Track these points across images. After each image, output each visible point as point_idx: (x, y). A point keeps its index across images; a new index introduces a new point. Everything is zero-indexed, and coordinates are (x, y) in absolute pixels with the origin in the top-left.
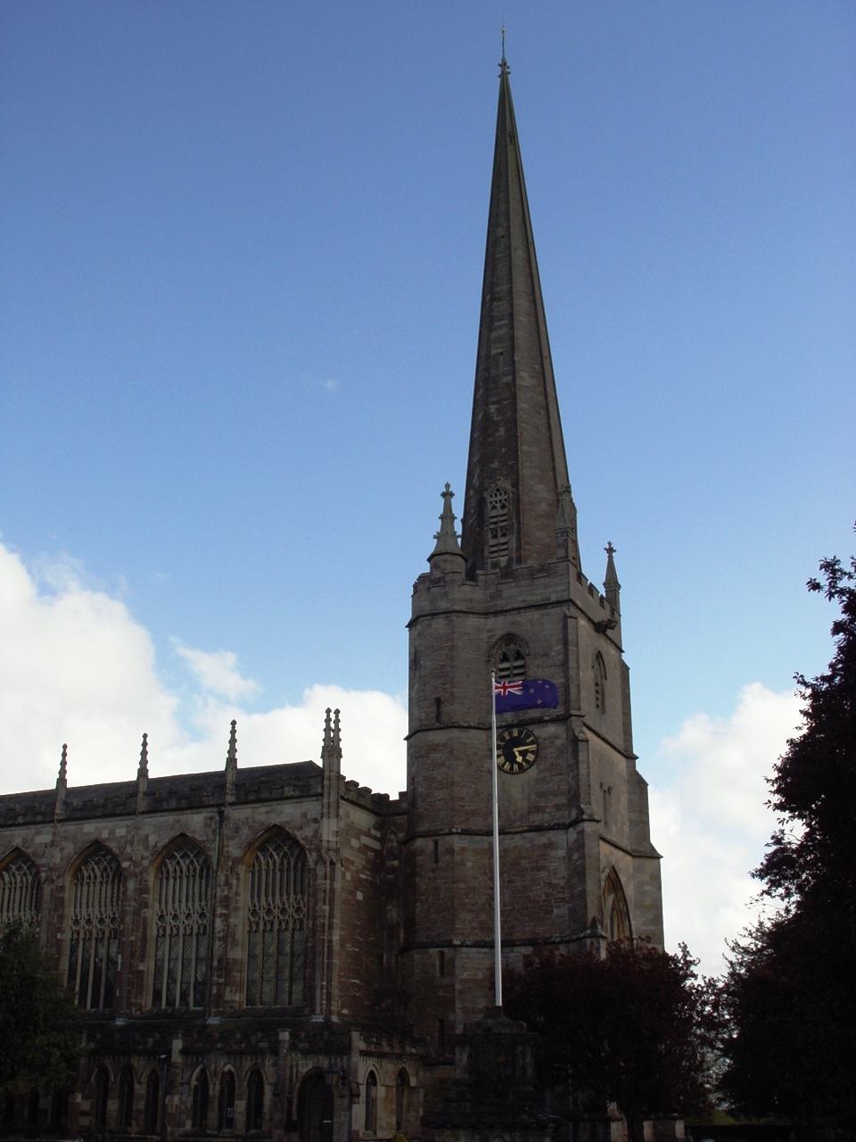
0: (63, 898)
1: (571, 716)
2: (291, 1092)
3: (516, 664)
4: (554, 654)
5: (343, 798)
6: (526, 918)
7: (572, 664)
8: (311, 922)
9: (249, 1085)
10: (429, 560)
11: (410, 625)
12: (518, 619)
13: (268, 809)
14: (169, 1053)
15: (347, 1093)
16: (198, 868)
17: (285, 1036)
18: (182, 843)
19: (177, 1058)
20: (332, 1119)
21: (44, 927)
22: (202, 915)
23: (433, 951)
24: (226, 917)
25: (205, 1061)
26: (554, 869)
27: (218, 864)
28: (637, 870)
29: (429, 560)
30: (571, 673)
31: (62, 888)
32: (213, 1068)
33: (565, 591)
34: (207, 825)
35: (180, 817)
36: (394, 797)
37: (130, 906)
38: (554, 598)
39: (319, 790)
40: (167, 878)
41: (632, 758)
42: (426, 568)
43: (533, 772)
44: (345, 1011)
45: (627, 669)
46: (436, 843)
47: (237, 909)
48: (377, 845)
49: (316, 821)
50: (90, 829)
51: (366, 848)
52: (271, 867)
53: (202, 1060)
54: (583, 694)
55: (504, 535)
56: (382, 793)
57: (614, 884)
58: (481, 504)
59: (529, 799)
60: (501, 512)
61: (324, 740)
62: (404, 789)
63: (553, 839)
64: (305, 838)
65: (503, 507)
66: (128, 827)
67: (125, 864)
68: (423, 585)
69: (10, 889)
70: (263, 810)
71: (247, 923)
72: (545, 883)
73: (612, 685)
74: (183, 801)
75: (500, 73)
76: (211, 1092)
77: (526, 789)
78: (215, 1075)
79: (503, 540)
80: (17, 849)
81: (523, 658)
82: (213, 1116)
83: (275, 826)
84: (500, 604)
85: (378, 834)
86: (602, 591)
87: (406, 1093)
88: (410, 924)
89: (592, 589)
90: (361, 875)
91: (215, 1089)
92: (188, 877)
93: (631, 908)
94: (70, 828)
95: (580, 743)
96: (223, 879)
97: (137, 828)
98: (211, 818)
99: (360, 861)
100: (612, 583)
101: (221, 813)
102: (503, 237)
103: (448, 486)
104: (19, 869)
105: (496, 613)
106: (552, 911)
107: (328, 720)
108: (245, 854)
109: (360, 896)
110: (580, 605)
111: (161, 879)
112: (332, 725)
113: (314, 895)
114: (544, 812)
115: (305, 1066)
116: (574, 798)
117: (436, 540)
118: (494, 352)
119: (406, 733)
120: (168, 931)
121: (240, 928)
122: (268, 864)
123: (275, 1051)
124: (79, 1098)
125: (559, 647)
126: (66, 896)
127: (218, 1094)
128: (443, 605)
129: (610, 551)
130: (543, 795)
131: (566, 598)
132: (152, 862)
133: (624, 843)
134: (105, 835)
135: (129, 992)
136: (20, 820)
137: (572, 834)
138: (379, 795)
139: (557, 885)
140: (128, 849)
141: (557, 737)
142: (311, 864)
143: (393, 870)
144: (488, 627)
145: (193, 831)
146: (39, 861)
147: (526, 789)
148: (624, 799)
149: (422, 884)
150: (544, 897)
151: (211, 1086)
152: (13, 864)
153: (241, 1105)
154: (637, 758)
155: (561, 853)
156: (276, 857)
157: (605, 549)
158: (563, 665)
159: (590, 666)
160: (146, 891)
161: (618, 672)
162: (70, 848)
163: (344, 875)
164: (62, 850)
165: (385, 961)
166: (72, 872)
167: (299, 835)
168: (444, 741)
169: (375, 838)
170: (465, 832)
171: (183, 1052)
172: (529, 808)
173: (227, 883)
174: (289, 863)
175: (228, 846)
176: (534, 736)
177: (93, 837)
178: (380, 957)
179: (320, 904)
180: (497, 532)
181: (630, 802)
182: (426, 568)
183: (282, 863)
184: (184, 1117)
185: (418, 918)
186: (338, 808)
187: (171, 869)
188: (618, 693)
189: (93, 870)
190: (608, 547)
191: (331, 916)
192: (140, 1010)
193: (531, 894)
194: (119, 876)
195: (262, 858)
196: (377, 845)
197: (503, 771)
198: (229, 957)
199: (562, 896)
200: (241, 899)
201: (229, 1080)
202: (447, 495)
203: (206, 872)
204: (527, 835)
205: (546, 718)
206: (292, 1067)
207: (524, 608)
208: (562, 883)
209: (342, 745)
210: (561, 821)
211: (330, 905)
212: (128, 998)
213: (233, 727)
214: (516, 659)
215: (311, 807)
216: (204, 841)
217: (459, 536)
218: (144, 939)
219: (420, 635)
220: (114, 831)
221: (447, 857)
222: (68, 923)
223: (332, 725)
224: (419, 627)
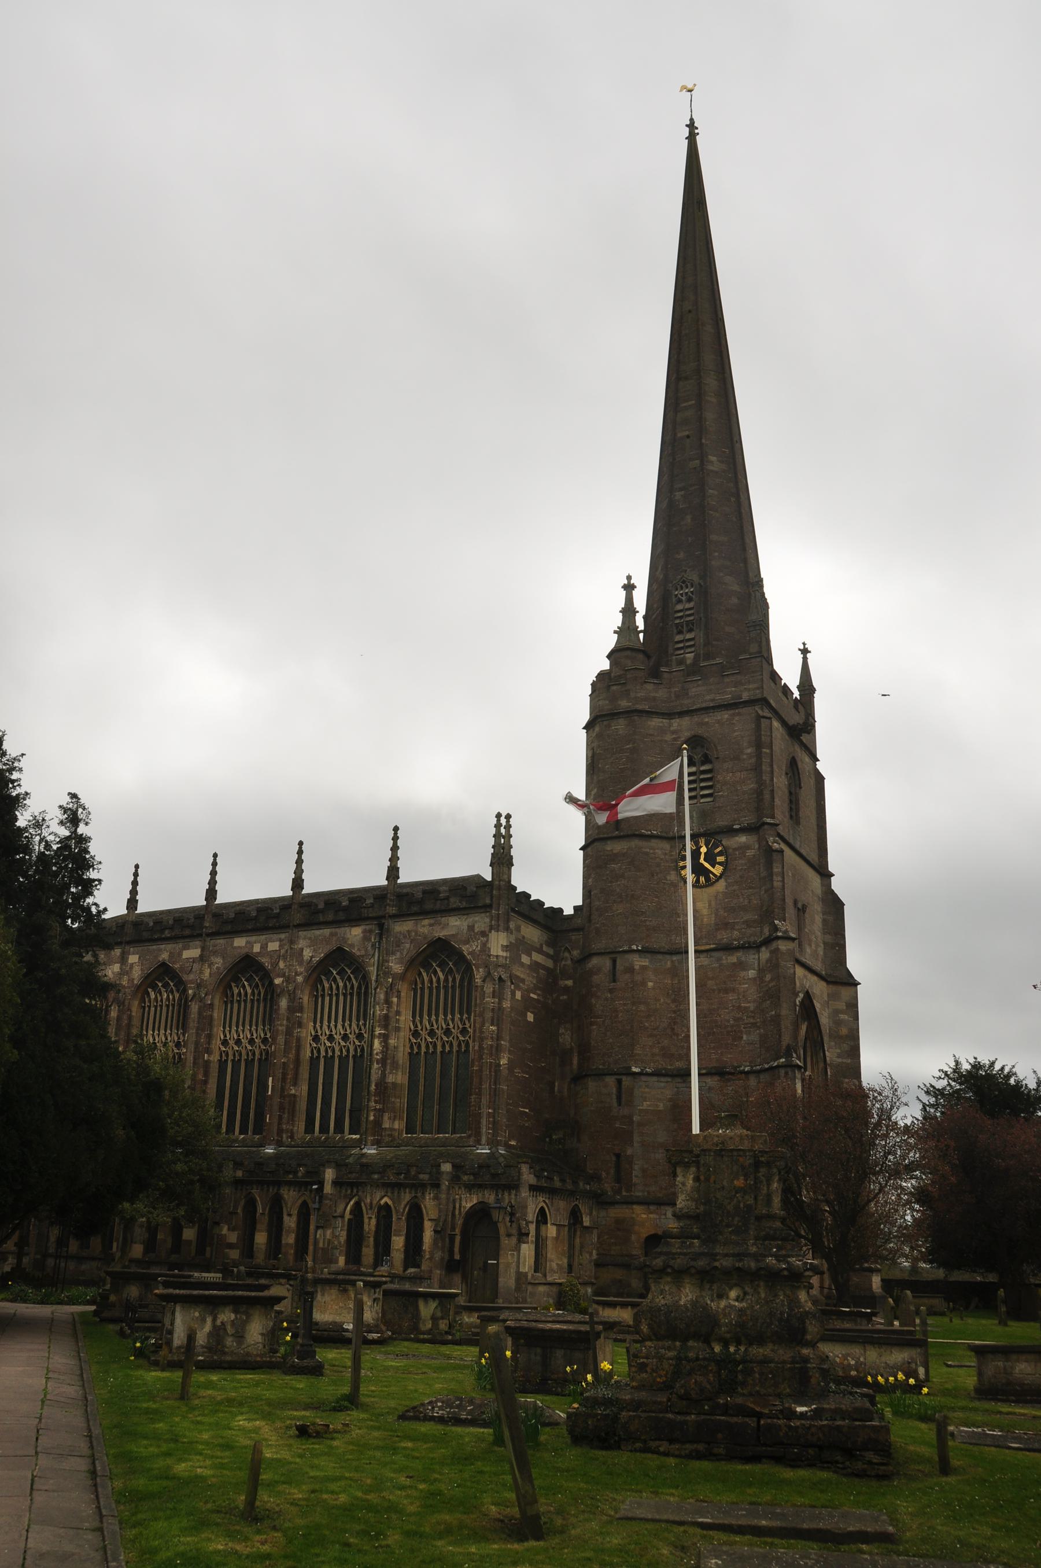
0: (211, 1016)
1: (765, 824)
2: (453, 1229)
3: (703, 768)
4: (745, 757)
5: (513, 910)
6: (712, 1045)
7: (765, 768)
8: (477, 1044)
9: (408, 1220)
10: (608, 657)
11: (588, 727)
12: (706, 720)
13: (432, 921)
14: (321, 1184)
15: (514, 1231)
16: (356, 985)
17: (446, 1167)
19: (328, 1189)
20: (498, 1260)
21: (192, 1047)
22: (360, 1037)
23: (611, 1080)
24: (385, 1038)
25: (360, 1193)
27: (376, 981)
28: (832, 996)
29: (608, 657)
30: (764, 778)
31: (211, 1005)
32: (369, 1201)
33: (758, 688)
34: (366, 938)
35: (337, 930)
36: (568, 911)
37: (281, 1025)
38: (745, 696)
39: (488, 901)
40: (323, 996)
41: (826, 875)
42: (606, 665)
43: (721, 885)
44: (513, 1143)
45: (823, 778)
46: (614, 961)
47: (398, 1029)
48: (549, 964)
49: (484, 934)
50: (240, 942)
51: (535, 966)
52: (435, 985)
53: (357, 1192)
54: (777, 802)
55: (690, 631)
56: (556, 906)
57: (808, 1010)
59: (716, 915)
60: (688, 606)
61: (493, 847)
62: (580, 903)
63: (743, 959)
64: (471, 953)
65: (690, 600)
66: (281, 940)
67: (278, 981)
68: (602, 684)
69: (156, 1007)
70: (426, 922)
71: (408, 1045)
72: (733, 1006)
73: (806, 795)
74: (341, 913)
75: (687, 135)
76: (366, 1227)
78: (371, 1208)
79: (689, 636)
80: (164, 964)
81: (710, 762)
82: (368, 1252)
83: (439, 939)
84: (686, 703)
85: (551, 952)
86: (796, 694)
87: (578, 1233)
88: (584, 1049)
89: (786, 690)
90: (532, 995)
91: (370, 1224)
92: (345, 995)
93: (826, 1039)
94: (221, 942)
95: (775, 854)
96: (382, 996)
97: (292, 942)
98: (371, 931)
99: (531, 979)
101: (381, 926)
102: (690, 311)
103: (629, 578)
104: (166, 985)
105: (681, 714)
107: (498, 826)
108: (406, 970)
109: (530, 1017)
110: (774, 705)
111: (317, 997)
112: (503, 831)
113: (481, 1015)
114: (733, 929)
115: (469, 1202)
116: (768, 913)
117: (616, 635)
118: (679, 435)
119: (583, 843)
120: (323, 1053)
121: (401, 1049)
122: (431, 981)
123: (437, 1186)
124: (225, 1230)
126: (215, 1015)
127: (373, 1228)
128: (624, 704)
129: (805, 651)
131: (759, 696)
132: (307, 979)
133: (818, 966)
134: (257, 948)
135: (280, 1118)
136: (167, 934)
137: (765, 954)
138: (551, 908)
140: (282, 965)
141: (747, 847)
142: (478, 980)
143: (566, 990)
144: (672, 729)
146: (185, 977)
147: (713, 903)
148: (818, 919)
151: (366, 1221)
152: (160, 981)
153: (398, 1242)
154: (833, 875)
155: (752, 973)
156: (440, 974)
157: (800, 650)
158: (756, 769)
159: (784, 773)
160: (301, 1009)
161: (812, 782)
162: (218, 962)
163: (513, 994)
164: (210, 966)
165: (556, 1088)
166: (221, 989)
167: (465, 949)
169: (547, 955)
170: (645, 951)
171: (336, 1183)
173: (387, 1001)
174: (454, 979)
175: (388, 962)
176: (722, 845)
177: (244, 951)
178: (552, 1085)
179: (487, 1025)
180: (682, 627)
181: (825, 922)
182: (606, 665)
183: (446, 980)
184: (337, 1252)
185: (593, 1043)
186: (508, 921)
187: (327, 985)
188: (812, 804)
189: (244, 987)
190: (802, 647)
191: (499, 1038)
192: (292, 1137)
193: (718, 1018)
194: (271, 994)
195: (424, 974)
196: (549, 964)
199: (752, 1020)
200: (402, 1018)
201: (385, 1214)
202: (629, 588)
203: (364, 993)
204: (716, 954)
205: (736, 827)
206: (454, 1201)
207: (713, 708)
208: (752, 1006)
209: (513, 852)
210: (752, 939)
211: (498, 1025)
212: (279, 1124)
213: (396, 833)
214: (703, 763)
215: (481, 921)
216: (363, 956)
217: (641, 631)
218: (297, 1061)
219: (599, 736)
220: (267, 944)
221: (627, 976)
222: (216, 1043)
223: (503, 831)
224: (597, 729)
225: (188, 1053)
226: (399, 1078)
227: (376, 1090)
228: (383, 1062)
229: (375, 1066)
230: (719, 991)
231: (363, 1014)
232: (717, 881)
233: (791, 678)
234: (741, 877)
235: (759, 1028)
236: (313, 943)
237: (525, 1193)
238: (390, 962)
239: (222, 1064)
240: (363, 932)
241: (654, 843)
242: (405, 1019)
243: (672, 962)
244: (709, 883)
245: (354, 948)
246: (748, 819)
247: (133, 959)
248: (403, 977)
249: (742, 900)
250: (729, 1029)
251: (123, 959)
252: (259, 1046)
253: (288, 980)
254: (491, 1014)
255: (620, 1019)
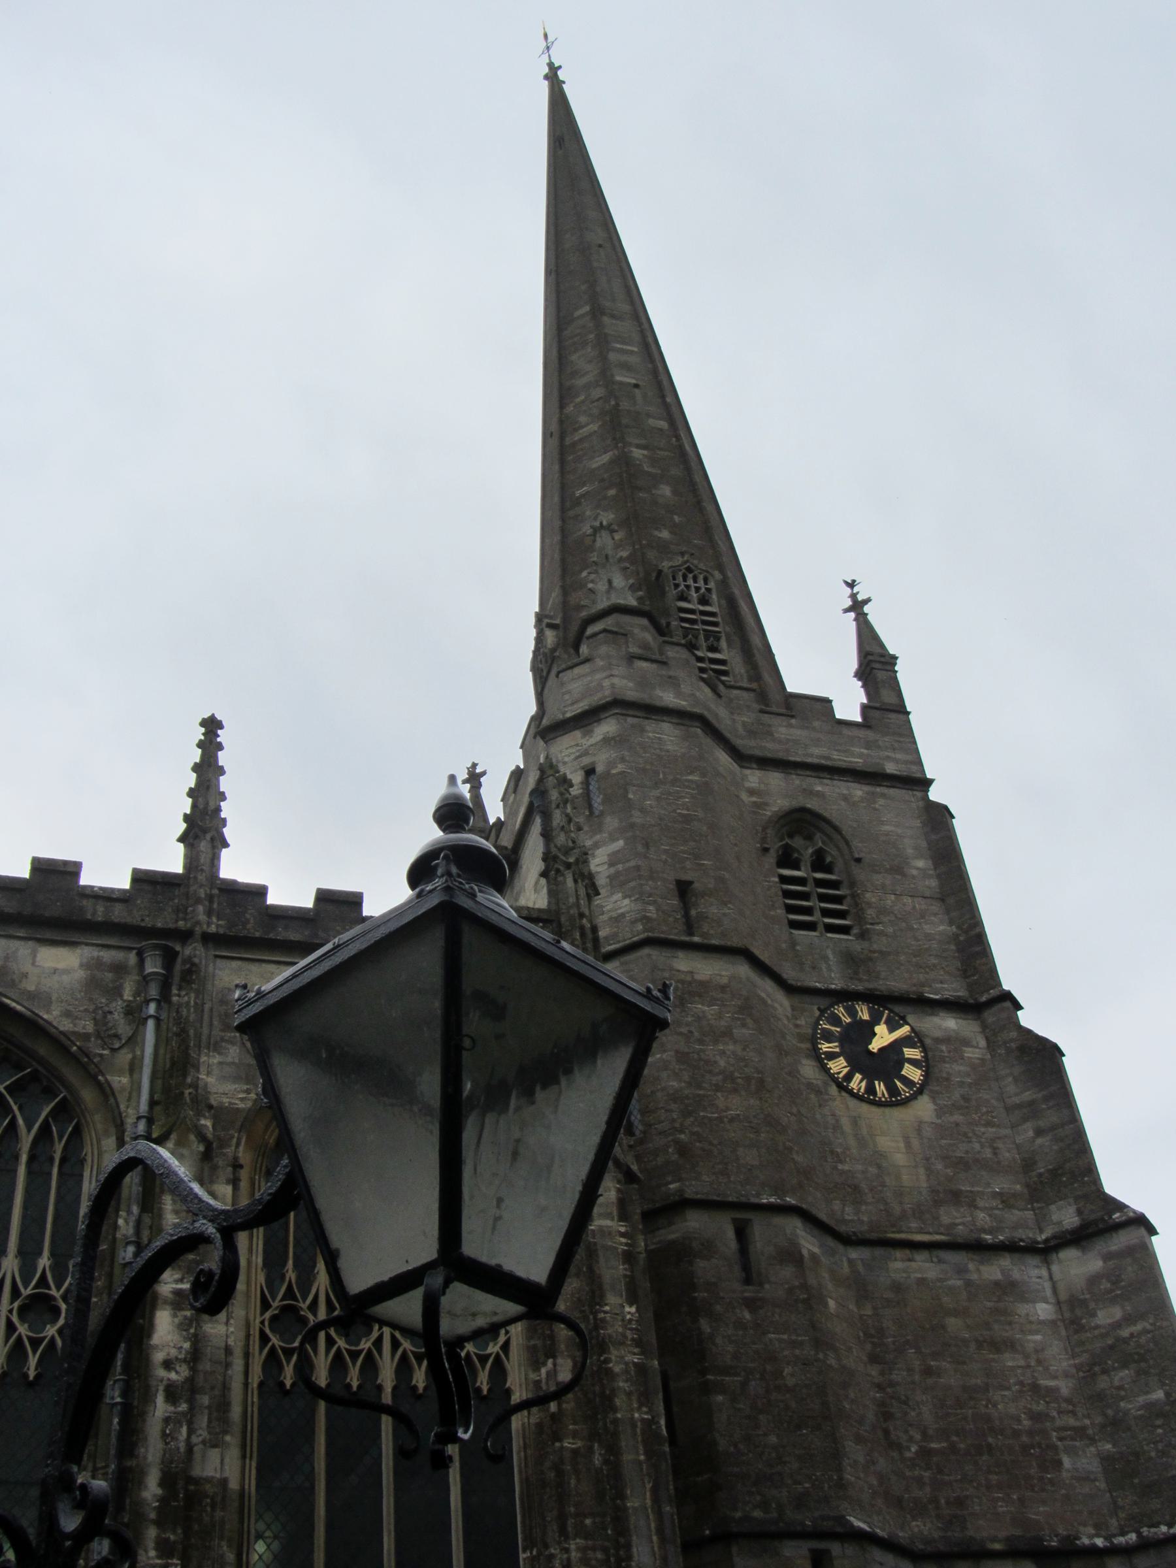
4: (915, 872)
6: (994, 1478)
12: (819, 788)
26: (1036, 1351)
43: (924, 1108)
63: (1016, 1275)
72: (1021, 1383)
77: (915, 1143)
98: (119, 969)
105: (766, 763)
106: (1059, 1464)
114: (973, 1205)
130: (963, 1164)
139: (1052, 1392)
145: (32, 996)
147: (915, 1143)
149: (719, 1340)
150: (1027, 1423)
168: (725, 981)
172: (933, 1191)
197: (850, 1092)
198: (197, 1472)
199: (1072, 1422)
208: (1065, 1387)
216: (86, 1037)
221: (787, 1272)
227: (164, 1501)
229: (161, 1407)
230: (980, 1344)
232: (913, 1097)
234: (965, 1099)
235: (1092, 1441)
238: (203, 1069)
240: (85, 966)
243: (850, 1261)
244: (895, 1101)
245: (47, 1006)
249: (977, 1146)
250: (1025, 1439)
254: (621, 1269)
255: (790, 1382)
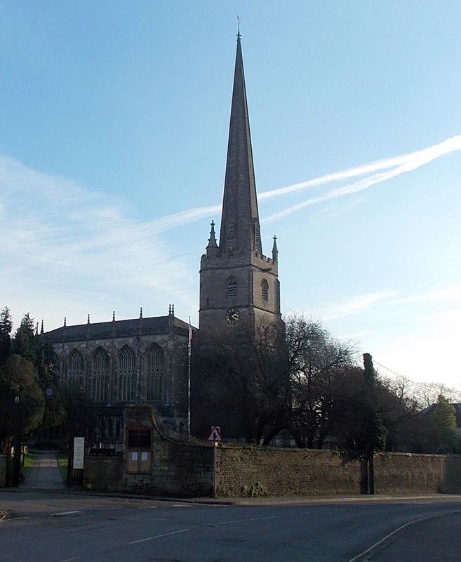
18: (126, 347)
22: (133, 371)
24: (140, 372)
31: (90, 362)
58: (225, 226)
73: (271, 290)
94: (92, 342)
100: (275, 251)
107: (170, 308)
118: (231, 166)
125: (247, 281)
129: (275, 238)
134: (103, 344)
173: (140, 361)
202: (213, 224)
215: (166, 337)
225: (84, 376)
226: (144, 384)
228: (140, 380)
231: (134, 365)
233: (267, 252)
236: (119, 343)
237: (175, 418)
239: (95, 379)
241: (218, 310)
242: (146, 365)
246: (246, 303)
247: (66, 347)
248: (145, 354)
251: (63, 347)
252: (105, 374)
253: (112, 354)
